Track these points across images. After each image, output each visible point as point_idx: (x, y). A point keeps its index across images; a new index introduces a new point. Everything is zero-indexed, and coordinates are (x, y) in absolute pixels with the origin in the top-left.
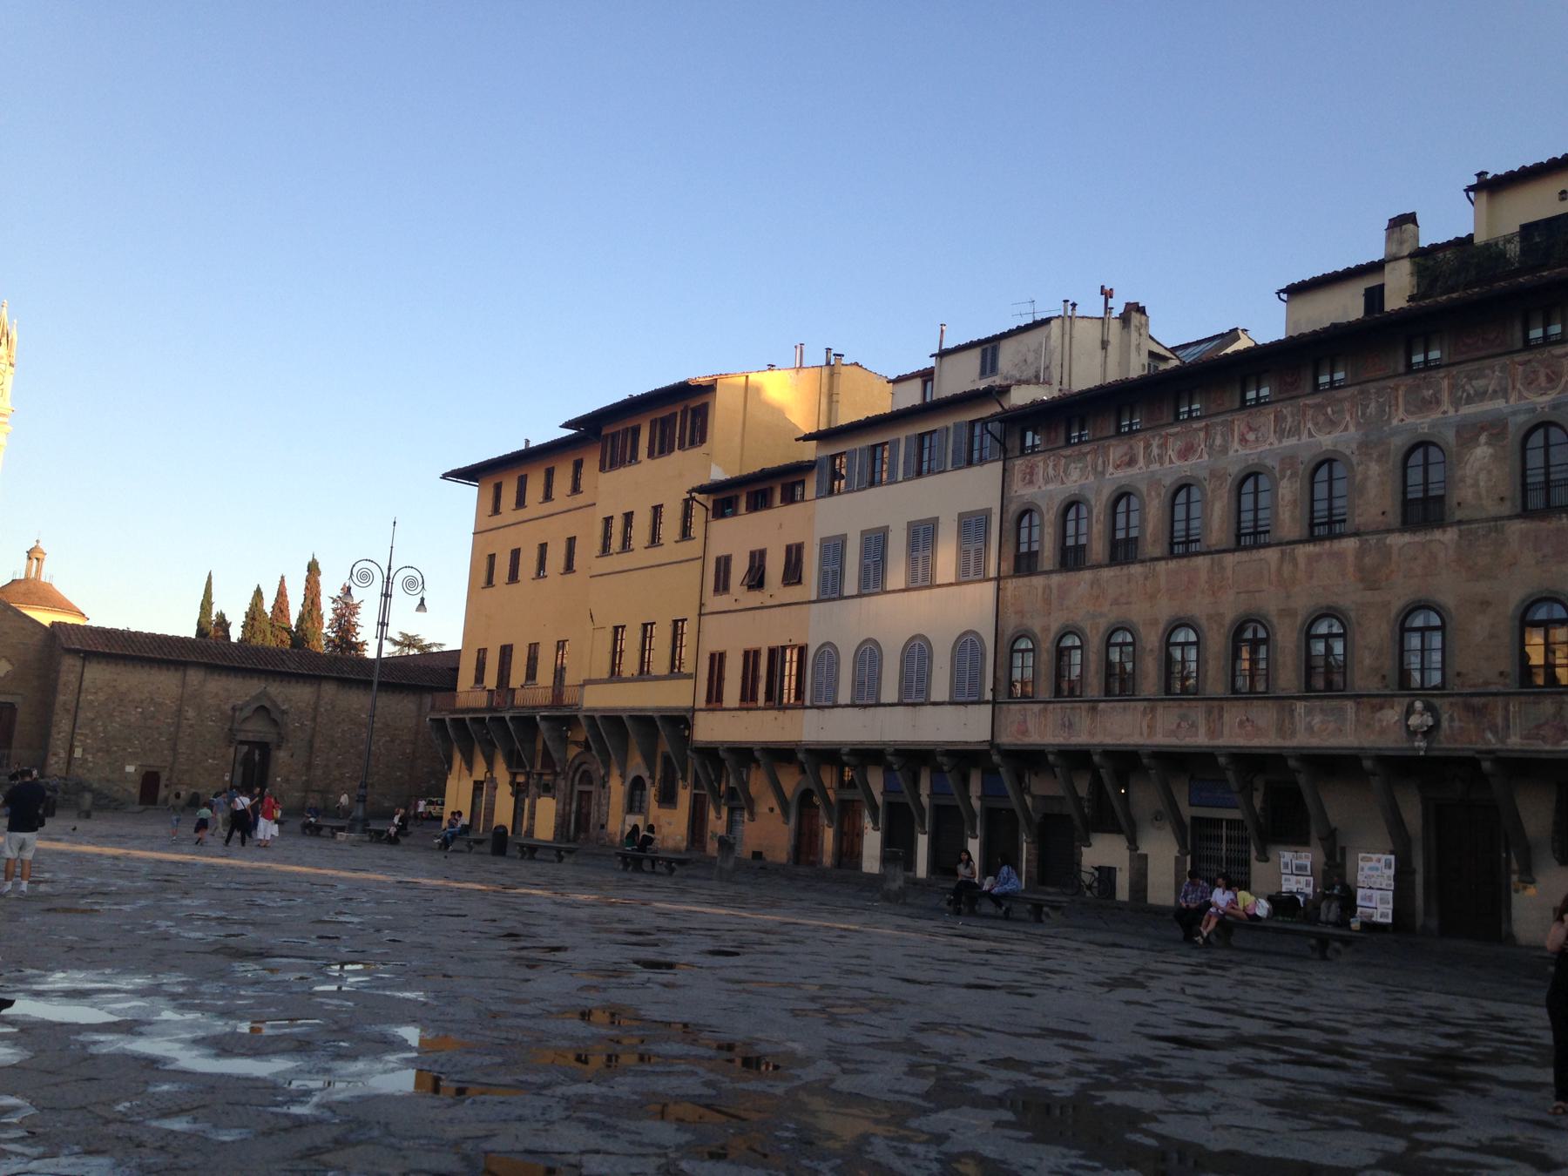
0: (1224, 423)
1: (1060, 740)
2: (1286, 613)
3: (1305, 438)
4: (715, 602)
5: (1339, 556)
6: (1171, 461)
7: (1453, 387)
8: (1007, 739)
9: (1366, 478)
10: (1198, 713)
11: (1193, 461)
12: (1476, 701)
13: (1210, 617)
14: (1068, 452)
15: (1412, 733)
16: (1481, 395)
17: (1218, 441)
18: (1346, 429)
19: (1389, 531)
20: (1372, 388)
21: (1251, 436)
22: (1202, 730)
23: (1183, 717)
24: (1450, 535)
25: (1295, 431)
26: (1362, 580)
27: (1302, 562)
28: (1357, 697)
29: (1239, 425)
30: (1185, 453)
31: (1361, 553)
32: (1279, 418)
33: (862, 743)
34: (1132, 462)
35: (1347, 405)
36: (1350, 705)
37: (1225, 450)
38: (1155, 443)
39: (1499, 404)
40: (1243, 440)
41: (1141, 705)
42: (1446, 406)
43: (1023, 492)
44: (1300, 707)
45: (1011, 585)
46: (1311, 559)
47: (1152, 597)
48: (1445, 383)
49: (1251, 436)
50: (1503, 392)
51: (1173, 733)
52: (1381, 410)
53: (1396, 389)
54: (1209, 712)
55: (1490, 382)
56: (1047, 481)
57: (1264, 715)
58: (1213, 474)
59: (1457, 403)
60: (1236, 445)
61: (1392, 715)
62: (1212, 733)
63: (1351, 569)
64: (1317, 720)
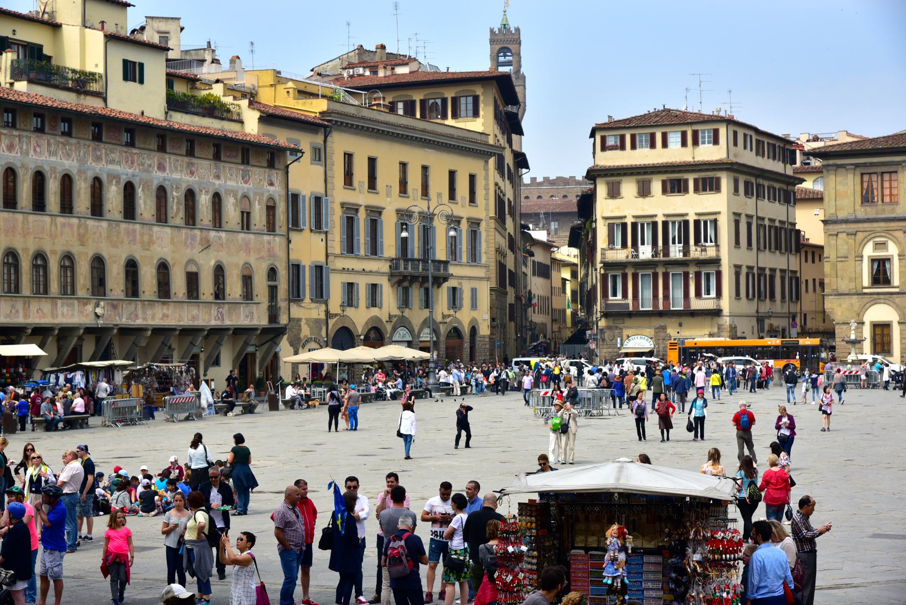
0: (27, 137)
2: (54, 252)
3: (59, 160)
7: (106, 154)
9: (80, 189)
11: (13, 154)
12: (115, 302)
13: (23, 250)
15: (97, 316)
16: (112, 162)
17: (24, 147)
20: (82, 142)
21: (38, 149)
22: (21, 314)
23: (13, 307)
24: (104, 224)
25: (55, 154)
26: (79, 240)
27: (59, 225)
28: (78, 299)
29: (34, 138)
30: (10, 148)
31: (79, 226)
32: (49, 144)
35: (73, 148)
36: (76, 302)
37: (27, 153)
40: (35, 150)
42: (104, 162)
44: (59, 302)
46: (63, 225)
48: (104, 151)
49: (38, 149)
50: (119, 163)
51: (7, 316)
52: (84, 153)
53: (89, 146)
54: (24, 304)
55: (115, 156)
57: (46, 306)
58: (23, 166)
59: (107, 162)
60: (32, 152)
61: (90, 308)
62: (26, 316)
63: (76, 234)
64: (66, 309)
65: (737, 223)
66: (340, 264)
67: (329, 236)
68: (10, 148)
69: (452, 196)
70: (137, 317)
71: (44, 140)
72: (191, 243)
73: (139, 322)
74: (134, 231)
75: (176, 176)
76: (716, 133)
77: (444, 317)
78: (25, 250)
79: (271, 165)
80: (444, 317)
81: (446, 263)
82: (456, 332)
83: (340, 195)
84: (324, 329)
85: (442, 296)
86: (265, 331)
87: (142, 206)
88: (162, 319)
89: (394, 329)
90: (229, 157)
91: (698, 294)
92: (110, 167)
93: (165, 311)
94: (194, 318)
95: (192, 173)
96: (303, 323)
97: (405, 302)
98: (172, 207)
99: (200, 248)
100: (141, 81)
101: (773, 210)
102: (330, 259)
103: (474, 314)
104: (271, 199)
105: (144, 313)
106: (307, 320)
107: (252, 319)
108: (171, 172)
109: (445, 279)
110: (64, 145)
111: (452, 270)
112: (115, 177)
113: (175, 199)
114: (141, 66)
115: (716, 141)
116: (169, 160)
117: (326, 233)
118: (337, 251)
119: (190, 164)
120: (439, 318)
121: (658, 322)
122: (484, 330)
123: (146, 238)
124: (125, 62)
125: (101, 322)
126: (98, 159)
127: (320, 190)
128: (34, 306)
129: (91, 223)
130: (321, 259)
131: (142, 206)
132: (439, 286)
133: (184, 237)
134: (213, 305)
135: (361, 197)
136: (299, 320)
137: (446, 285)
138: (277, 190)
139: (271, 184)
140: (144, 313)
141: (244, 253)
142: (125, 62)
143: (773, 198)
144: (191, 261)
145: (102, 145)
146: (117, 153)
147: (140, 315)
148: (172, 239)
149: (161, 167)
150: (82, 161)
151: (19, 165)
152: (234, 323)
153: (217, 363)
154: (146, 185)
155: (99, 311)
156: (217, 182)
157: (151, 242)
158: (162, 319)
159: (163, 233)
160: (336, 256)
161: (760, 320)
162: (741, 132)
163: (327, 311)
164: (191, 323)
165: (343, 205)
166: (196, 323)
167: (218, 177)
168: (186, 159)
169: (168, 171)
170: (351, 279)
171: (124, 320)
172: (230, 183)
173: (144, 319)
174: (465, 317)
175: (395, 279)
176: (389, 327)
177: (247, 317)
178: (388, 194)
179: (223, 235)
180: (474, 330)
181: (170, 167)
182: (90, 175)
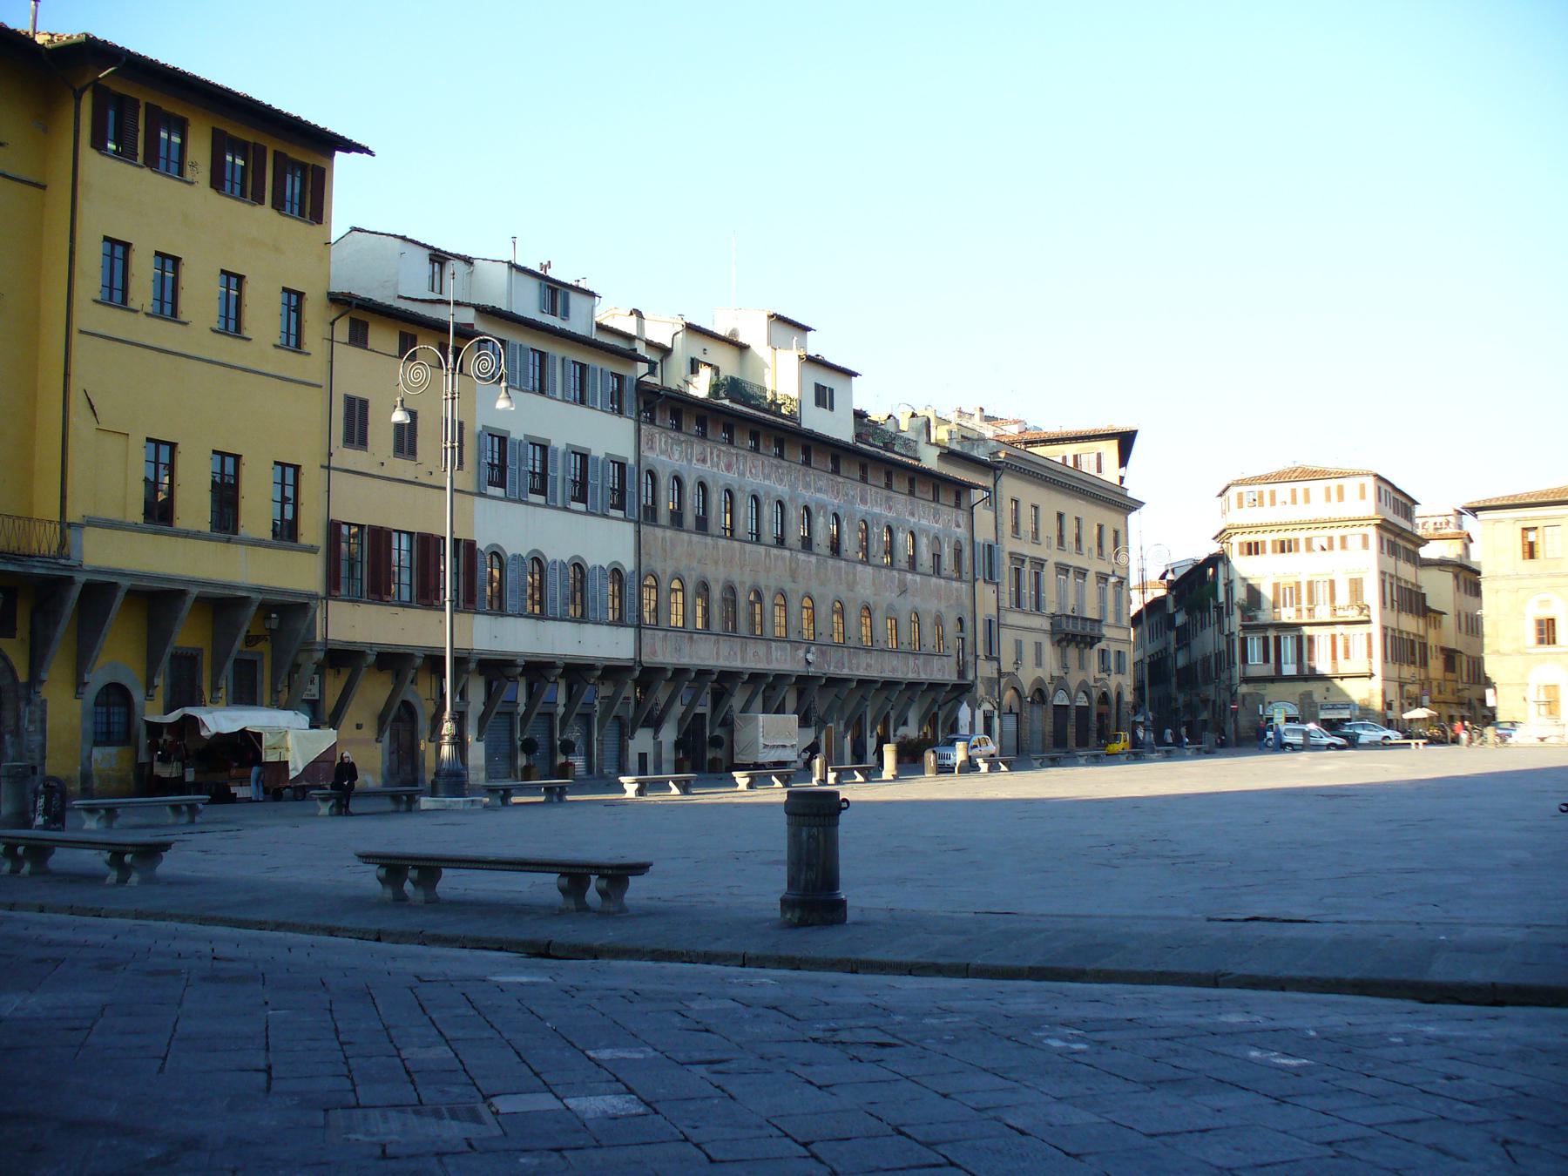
1: (675, 661)
4: (347, 457)
5: (783, 558)
10: (761, 648)
14: (672, 434)
15: (808, 663)
16: (819, 490)
24: (813, 559)
25: (767, 477)
30: (729, 467)
33: (537, 655)
34: (704, 461)
37: (744, 475)
39: (824, 497)
43: (652, 457)
45: (644, 529)
46: (777, 557)
47: (716, 563)
50: (826, 492)
51: (727, 659)
56: (662, 452)
65: (1383, 582)
66: (1012, 618)
68: (729, 467)
69: (1101, 554)
71: (759, 460)
73: (845, 672)
74: (840, 569)
75: (877, 510)
76: (1362, 488)
77: (1096, 680)
78: (742, 583)
79: (958, 506)
80: (1096, 680)
81: (1099, 621)
82: (1104, 698)
83: (1009, 545)
85: (1093, 655)
86: (955, 686)
89: (1055, 691)
91: (1347, 656)
92: (819, 495)
94: (894, 670)
95: (890, 508)
97: (1064, 666)
100: (832, 408)
101: (1407, 571)
103: (1119, 678)
104: (958, 542)
109: (1099, 640)
110: (778, 467)
111: (1106, 632)
112: (822, 506)
113: (879, 536)
114: (831, 391)
115: (1363, 497)
116: (871, 492)
119: (888, 499)
120: (1092, 683)
121: (1302, 687)
122: (1128, 697)
124: (818, 386)
125: (812, 669)
126: (807, 486)
127: (991, 538)
128: (752, 647)
129: (802, 557)
132: (1092, 646)
135: (1027, 549)
137: (1098, 646)
138: (962, 532)
139: (958, 526)
141: (935, 598)
142: (818, 386)
143: (1408, 560)
145: (811, 471)
146: (825, 480)
149: (863, 501)
150: (792, 486)
151: (736, 486)
153: (905, 723)
154: (851, 519)
155: (810, 657)
156: (912, 520)
159: (865, 572)
161: (1401, 686)
162: (1384, 487)
163: (999, 670)
165: (1011, 554)
167: (912, 514)
168: (885, 492)
171: (832, 670)
172: (924, 522)
174: (1113, 681)
175: (1058, 637)
176: (1051, 689)
178: (1049, 546)
179: (918, 578)
180: (1119, 695)
182: (801, 503)
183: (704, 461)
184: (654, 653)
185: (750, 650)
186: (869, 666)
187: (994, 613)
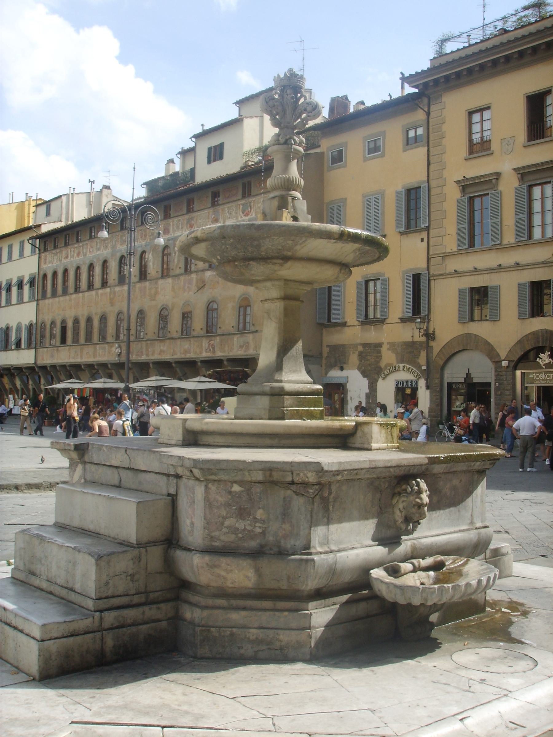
6: (241, 217)
8: (40, 362)
18: (252, 215)
19: (115, 286)
25: (98, 249)
38: (72, 250)
41: (68, 348)
46: (102, 294)
49: (91, 250)
62: (81, 357)
67: (432, 232)
70: (142, 354)
72: (188, 287)
84: (423, 354)
87: (152, 267)
88: (160, 354)
90: (228, 197)
93: (162, 348)
94: (186, 352)
96: (384, 350)
98: (174, 261)
99: (194, 288)
102: (433, 261)
105: (147, 350)
106: (392, 346)
107: (248, 348)
108: (174, 231)
117: (428, 229)
118: (451, 245)
123: (153, 291)
130: (420, 264)
131: (152, 267)
133: (182, 283)
134: (204, 339)
136: (380, 345)
140: (147, 350)
144: (187, 303)
147: (144, 352)
148: (173, 287)
152: (226, 354)
157: (157, 293)
158: (160, 354)
160: (445, 256)
164: (183, 356)
166: (188, 356)
169: (171, 233)
170: (479, 281)
173: (147, 355)
177: (241, 347)
181: (173, 228)
183: (67, 257)
184: (43, 359)
185: (85, 352)
186: (162, 352)
187: (422, 264)
